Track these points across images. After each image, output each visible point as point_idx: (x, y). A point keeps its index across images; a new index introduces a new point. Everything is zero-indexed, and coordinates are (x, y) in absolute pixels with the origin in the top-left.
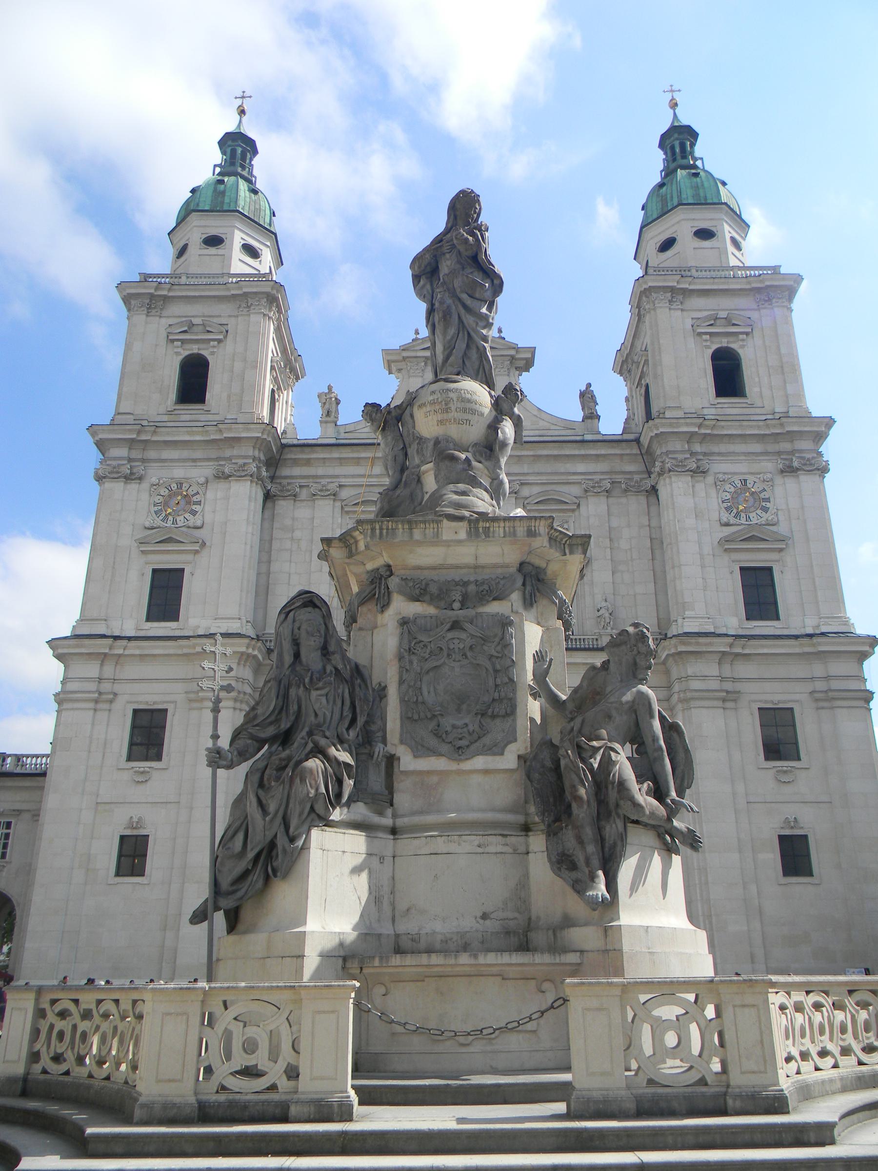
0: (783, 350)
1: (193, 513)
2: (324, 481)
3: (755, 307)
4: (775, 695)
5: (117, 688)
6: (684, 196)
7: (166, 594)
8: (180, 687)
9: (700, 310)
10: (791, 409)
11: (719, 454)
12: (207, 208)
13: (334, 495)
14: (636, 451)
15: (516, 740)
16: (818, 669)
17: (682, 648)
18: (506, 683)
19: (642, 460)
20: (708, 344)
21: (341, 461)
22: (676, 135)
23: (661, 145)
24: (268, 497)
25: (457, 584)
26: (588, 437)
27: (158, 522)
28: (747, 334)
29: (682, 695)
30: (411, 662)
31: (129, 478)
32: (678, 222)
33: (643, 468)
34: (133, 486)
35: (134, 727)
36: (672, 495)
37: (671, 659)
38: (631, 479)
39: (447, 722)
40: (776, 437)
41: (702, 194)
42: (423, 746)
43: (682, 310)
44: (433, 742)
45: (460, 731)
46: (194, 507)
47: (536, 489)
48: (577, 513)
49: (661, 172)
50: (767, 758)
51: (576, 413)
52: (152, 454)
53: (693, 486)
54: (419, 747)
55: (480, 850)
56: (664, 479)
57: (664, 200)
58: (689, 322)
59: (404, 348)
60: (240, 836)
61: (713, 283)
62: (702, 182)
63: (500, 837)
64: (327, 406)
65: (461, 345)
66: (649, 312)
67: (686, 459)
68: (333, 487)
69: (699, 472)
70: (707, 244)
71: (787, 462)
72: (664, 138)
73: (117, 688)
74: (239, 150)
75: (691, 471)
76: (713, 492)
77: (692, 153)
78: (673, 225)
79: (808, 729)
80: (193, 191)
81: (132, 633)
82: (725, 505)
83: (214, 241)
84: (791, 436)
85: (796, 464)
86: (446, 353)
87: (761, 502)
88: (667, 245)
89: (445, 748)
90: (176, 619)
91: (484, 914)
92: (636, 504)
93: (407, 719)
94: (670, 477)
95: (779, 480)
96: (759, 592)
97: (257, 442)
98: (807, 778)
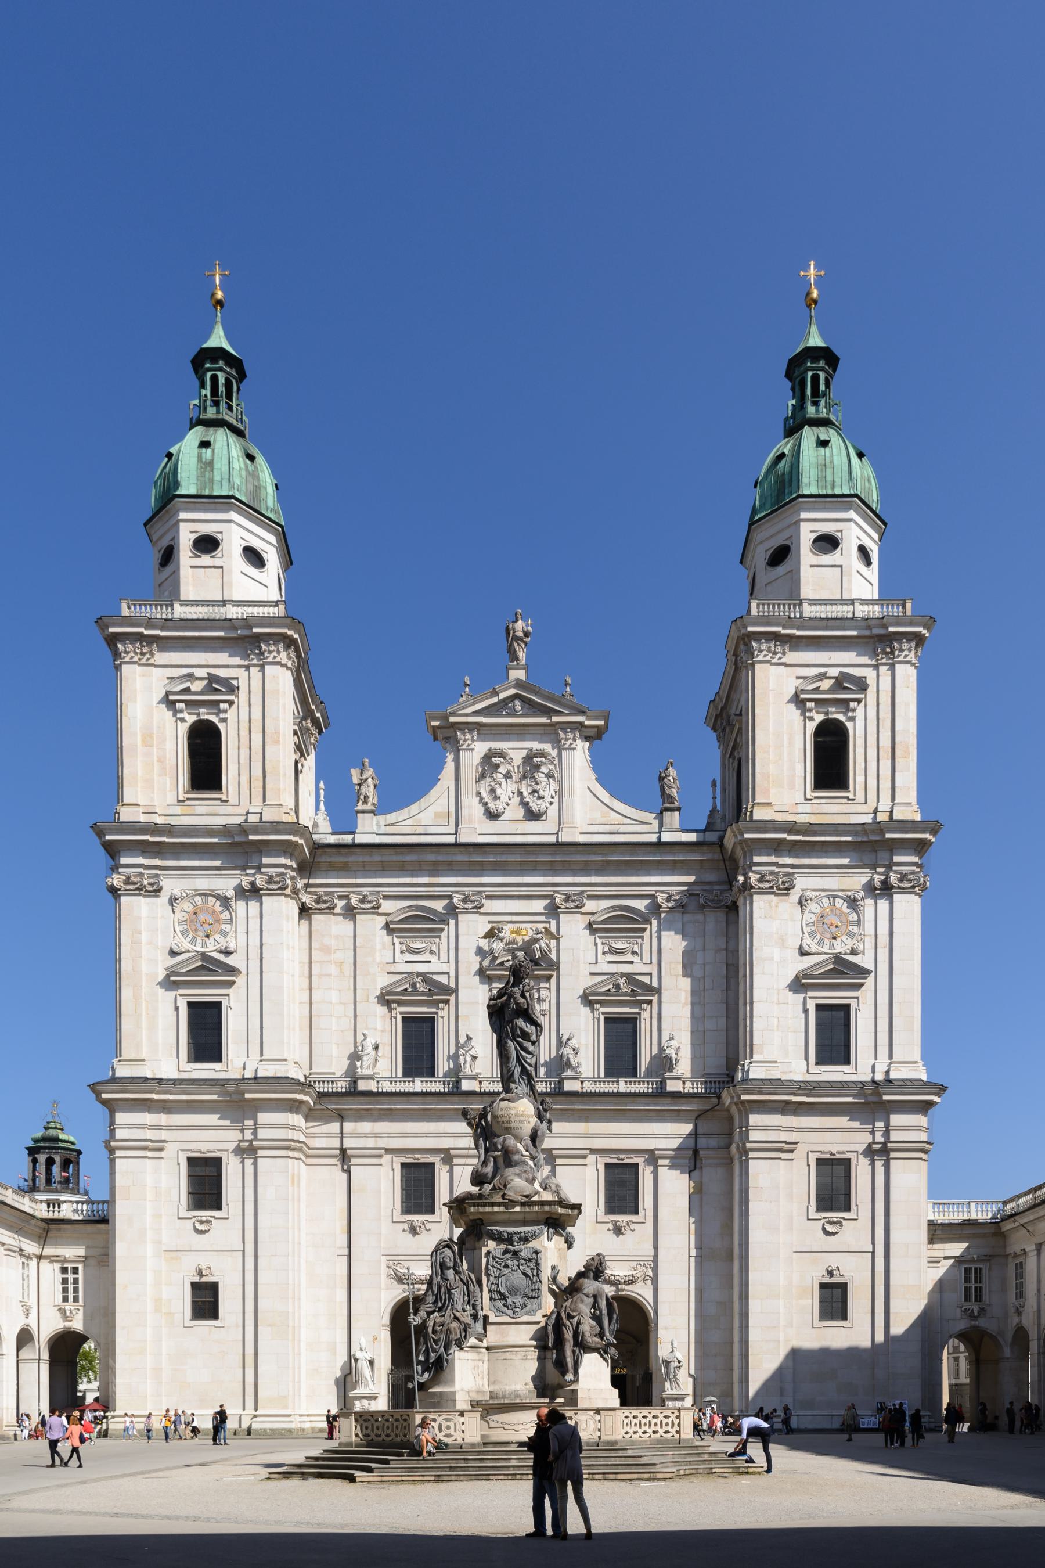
1: (225, 934)
10: (895, 808)
12: (193, 491)
14: (718, 856)
24: (304, 911)
27: (186, 944)
38: (710, 891)
41: (829, 478)
46: (223, 927)
50: (819, 1209)
62: (832, 456)
71: (883, 877)
74: (221, 380)
81: (175, 1075)
85: (893, 878)
90: (218, 1058)
92: (714, 921)
98: (856, 1228)
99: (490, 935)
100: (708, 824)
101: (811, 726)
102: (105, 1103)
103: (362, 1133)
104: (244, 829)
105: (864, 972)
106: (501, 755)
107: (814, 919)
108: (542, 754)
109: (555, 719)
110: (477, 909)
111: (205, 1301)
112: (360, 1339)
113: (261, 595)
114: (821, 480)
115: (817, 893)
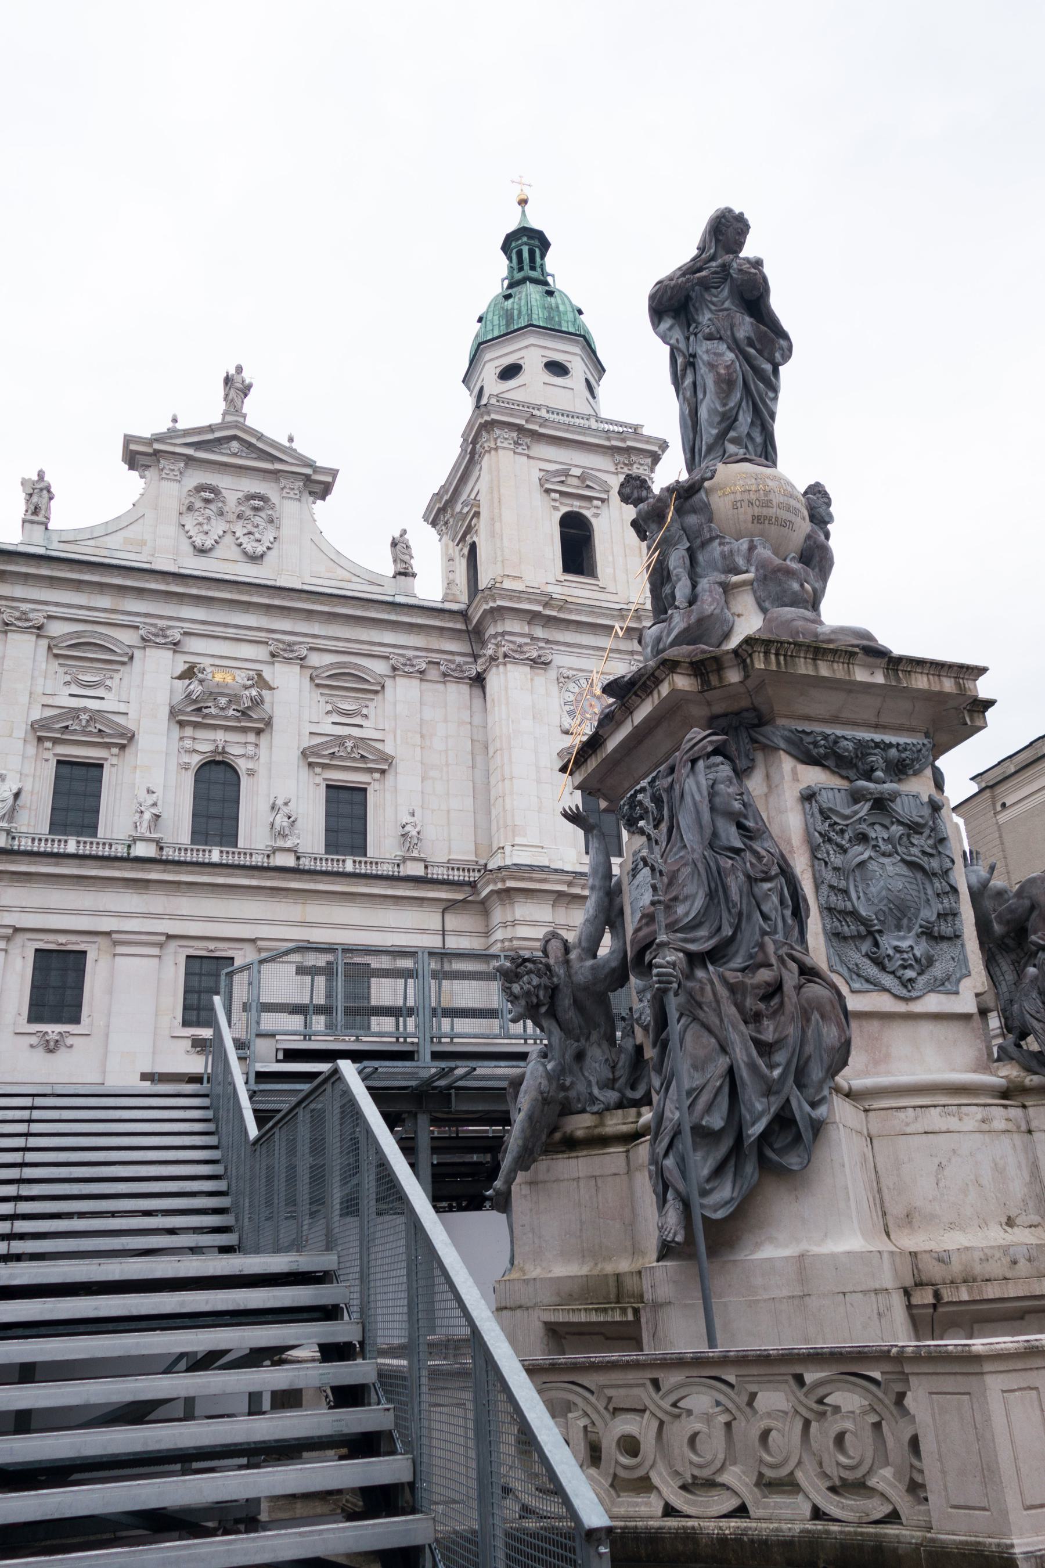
2: (24, 606)
3: (613, 469)
6: (535, 316)
9: (550, 461)
11: (564, 644)
13: (39, 628)
15: (969, 975)
17: (510, 884)
18: (947, 893)
20: (557, 504)
21: (53, 582)
22: (525, 239)
23: (506, 248)
25: (877, 745)
28: (603, 501)
29: (507, 944)
30: (828, 854)
32: (526, 347)
33: (469, 651)
36: (506, 688)
37: (495, 896)
39: (888, 942)
42: (858, 975)
43: (529, 457)
44: (872, 971)
45: (905, 956)
47: (329, 659)
48: (380, 696)
49: (503, 280)
51: (388, 569)
53: (532, 680)
54: (854, 977)
55: (985, 1127)
56: (497, 666)
57: (509, 316)
58: (536, 475)
59: (158, 438)
60: (724, 1102)
61: (567, 431)
63: (1001, 1109)
64: (35, 499)
65: (745, 419)
66: (489, 452)
67: (526, 644)
68: (38, 618)
69: (539, 663)
75: (531, 660)
76: (554, 689)
78: (520, 349)
82: (567, 708)
86: (724, 425)
88: (510, 372)
89: (888, 980)
91: (1009, 1218)
92: (458, 693)
93: (835, 937)
94: (505, 664)
99: (189, 673)
100: (446, 595)
101: (558, 515)
107: (572, 698)
109: (278, 466)
110: (176, 646)
115: (575, 673)
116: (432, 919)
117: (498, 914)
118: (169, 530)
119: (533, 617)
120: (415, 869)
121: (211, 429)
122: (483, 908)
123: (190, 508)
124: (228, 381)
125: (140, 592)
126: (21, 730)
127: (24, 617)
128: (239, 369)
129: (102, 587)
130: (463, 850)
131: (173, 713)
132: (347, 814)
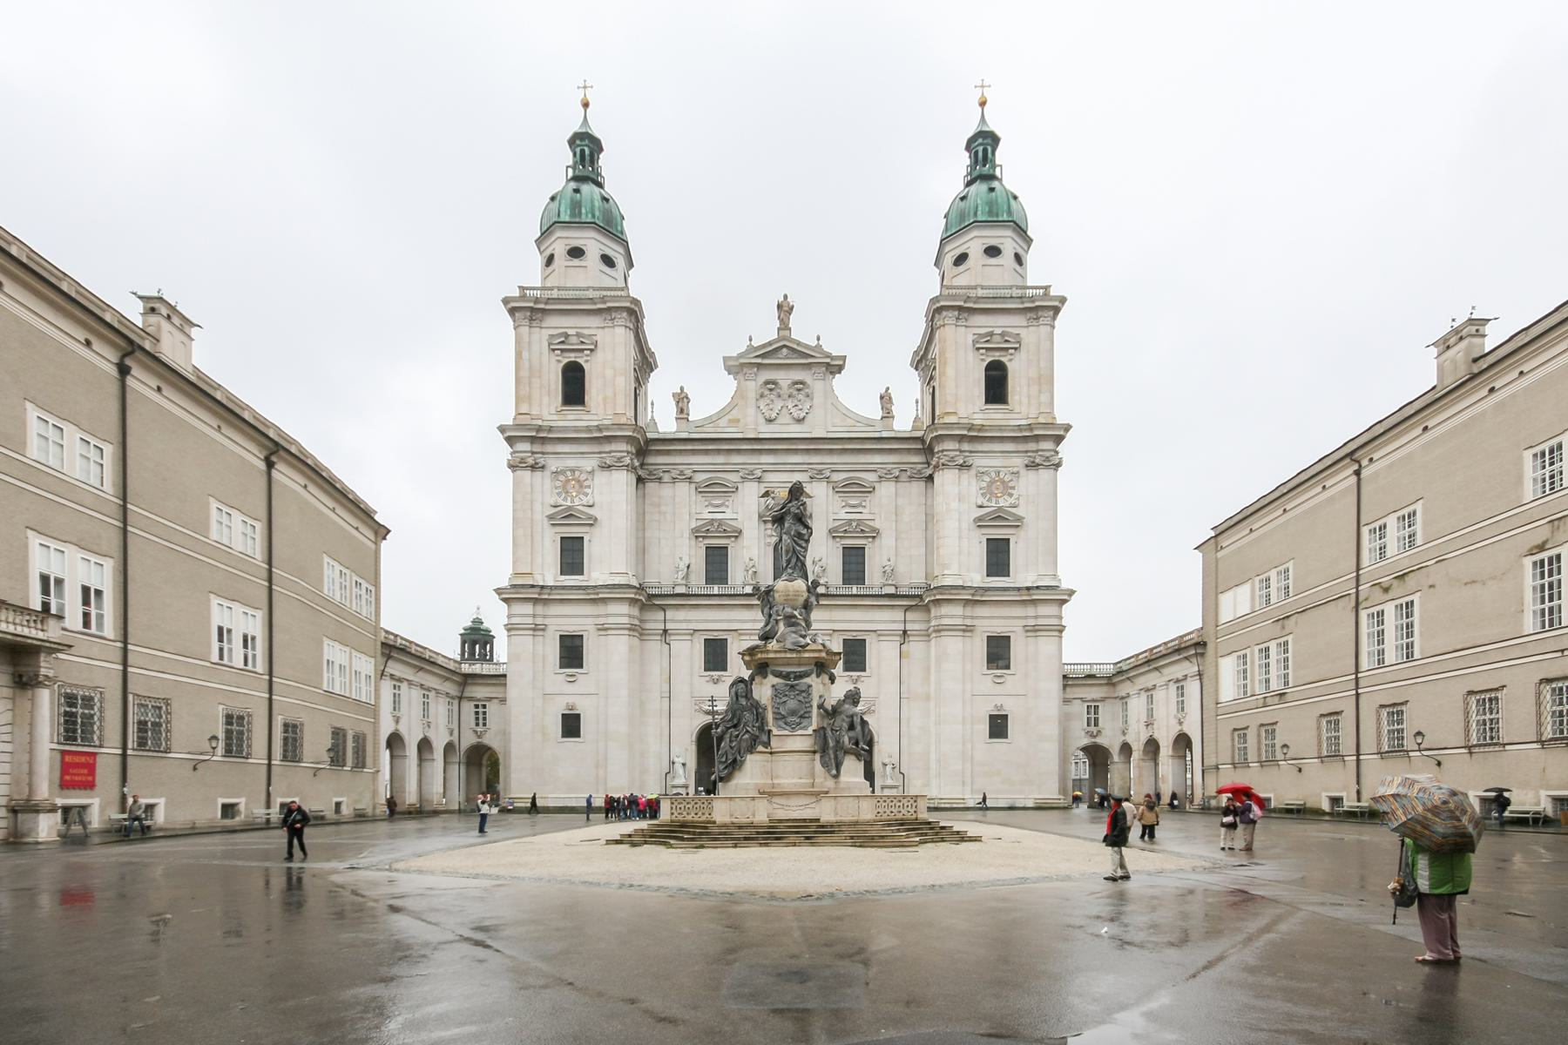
0: (1042, 365)
4: (998, 628)
5: (547, 621)
7: (572, 555)
8: (590, 621)
16: (1031, 611)
19: (926, 452)
21: (694, 452)
24: (640, 480)
26: (885, 435)
31: (533, 467)
34: (538, 474)
35: (561, 647)
40: (1025, 439)
51: (878, 414)
52: (549, 448)
59: (741, 356)
68: (688, 473)
69: (964, 467)
70: (993, 261)
72: (971, 141)
73: (547, 621)
77: (993, 161)
79: (1017, 650)
80: (553, 199)
83: (576, 253)
84: (1037, 438)
87: (1007, 489)
88: (961, 259)
95: (1023, 472)
96: (998, 557)
97: (629, 439)
98: (1014, 679)
99: (766, 494)
102: (505, 600)
103: (679, 619)
104: (599, 428)
105: (1020, 519)
106: (774, 383)
108: (801, 383)
111: (571, 725)
112: (675, 749)
113: (611, 284)
114: (990, 213)
116: (899, 615)
117: (934, 612)
118: (751, 411)
119: (961, 438)
120: (891, 590)
121: (770, 344)
122: (927, 608)
123: (762, 396)
124: (779, 306)
125: (739, 451)
126: (687, 534)
127: (682, 473)
128: (786, 297)
129: (719, 451)
130: (918, 578)
131: (760, 516)
132: (854, 563)
